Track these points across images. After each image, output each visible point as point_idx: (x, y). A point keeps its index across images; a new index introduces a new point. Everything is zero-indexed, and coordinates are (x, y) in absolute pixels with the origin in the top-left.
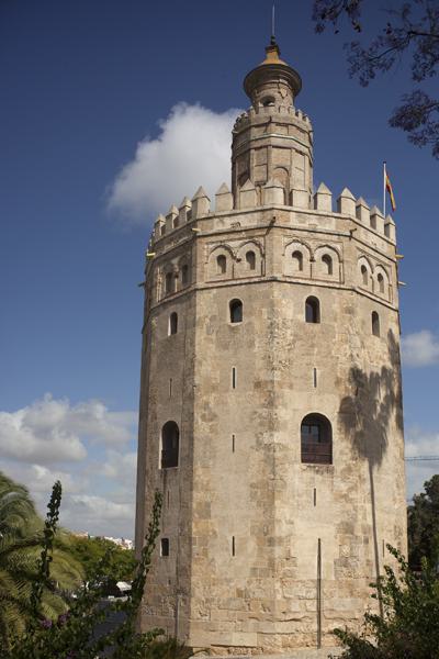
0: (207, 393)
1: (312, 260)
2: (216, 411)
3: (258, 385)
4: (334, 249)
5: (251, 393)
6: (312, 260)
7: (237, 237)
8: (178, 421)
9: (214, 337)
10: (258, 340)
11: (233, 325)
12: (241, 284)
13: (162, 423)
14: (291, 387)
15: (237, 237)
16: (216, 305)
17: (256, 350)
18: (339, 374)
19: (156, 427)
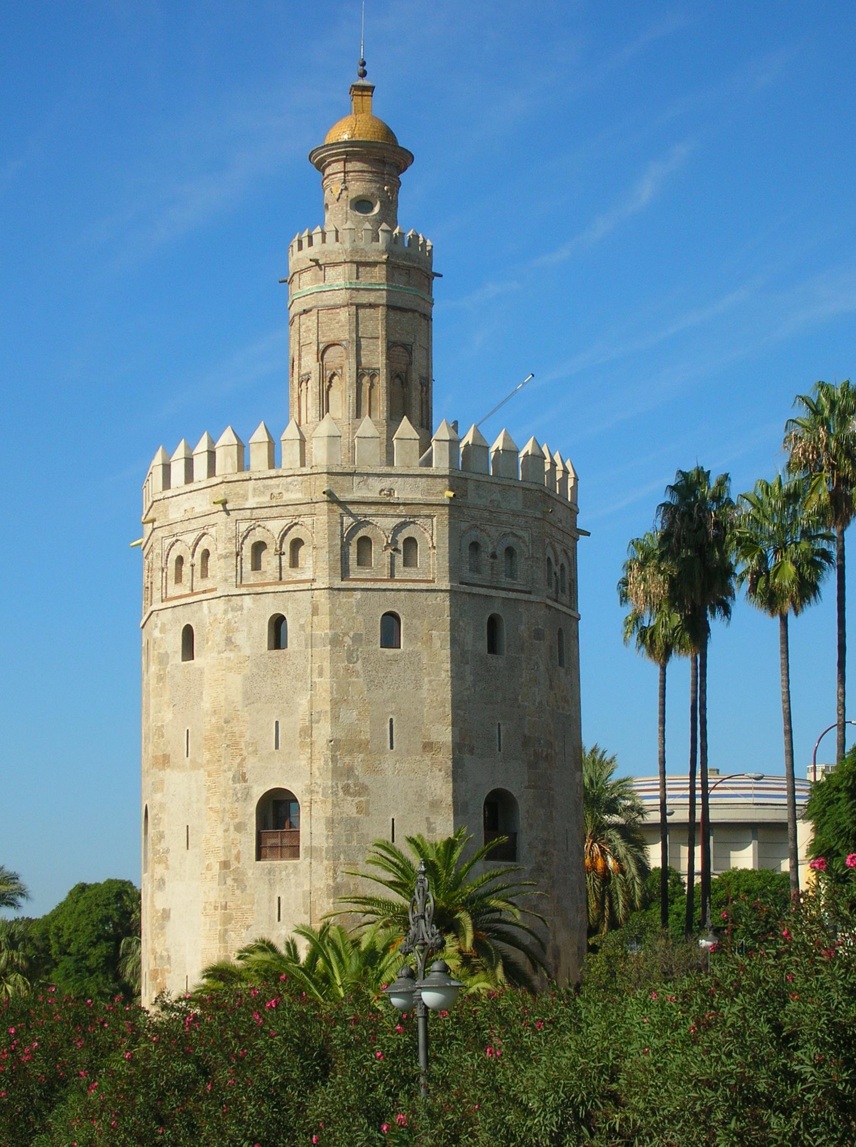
0: (350, 752)
1: (494, 556)
2: (365, 779)
3: (428, 746)
4: (520, 538)
5: (418, 758)
6: (494, 556)
7: (391, 512)
8: (296, 788)
9: (359, 666)
10: (426, 679)
11: (389, 652)
12: (399, 590)
13: (258, 792)
14: (471, 751)
15: (391, 512)
16: (360, 618)
17: (424, 693)
18: (526, 731)
19: (247, 795)
